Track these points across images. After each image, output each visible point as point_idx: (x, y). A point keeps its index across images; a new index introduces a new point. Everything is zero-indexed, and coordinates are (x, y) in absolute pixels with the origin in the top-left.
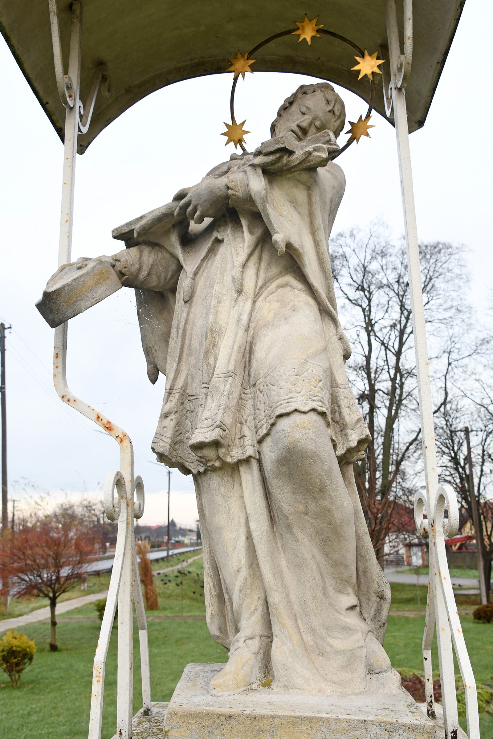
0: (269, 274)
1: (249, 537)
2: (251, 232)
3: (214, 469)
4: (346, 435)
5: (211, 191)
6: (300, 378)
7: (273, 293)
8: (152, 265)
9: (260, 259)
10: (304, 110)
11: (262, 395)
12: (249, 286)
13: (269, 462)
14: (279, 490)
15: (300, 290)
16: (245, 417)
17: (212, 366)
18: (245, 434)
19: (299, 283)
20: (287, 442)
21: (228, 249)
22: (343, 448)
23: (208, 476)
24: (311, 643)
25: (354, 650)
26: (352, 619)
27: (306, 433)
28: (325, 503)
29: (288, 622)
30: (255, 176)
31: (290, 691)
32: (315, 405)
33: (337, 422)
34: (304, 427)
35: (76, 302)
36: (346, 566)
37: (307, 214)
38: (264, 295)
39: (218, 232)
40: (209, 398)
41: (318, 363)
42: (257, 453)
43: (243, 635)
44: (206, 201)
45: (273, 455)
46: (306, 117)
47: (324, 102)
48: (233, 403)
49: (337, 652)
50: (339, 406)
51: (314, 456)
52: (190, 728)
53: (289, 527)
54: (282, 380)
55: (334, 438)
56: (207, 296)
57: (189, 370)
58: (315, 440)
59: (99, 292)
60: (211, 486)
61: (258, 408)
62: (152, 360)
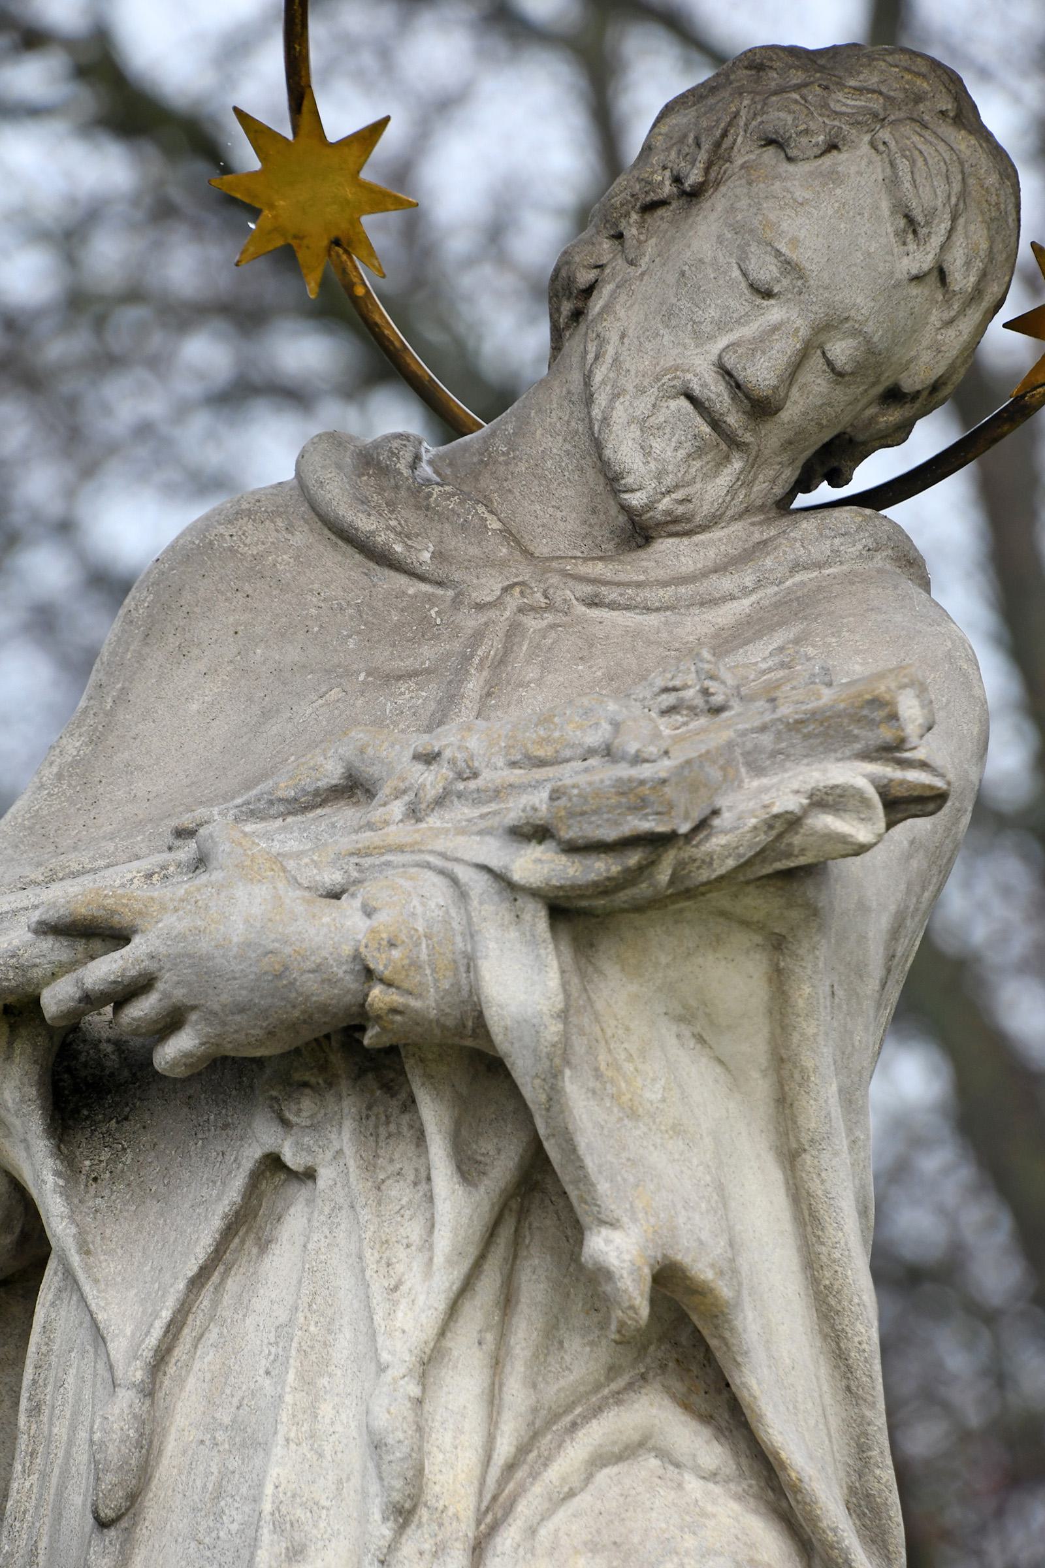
46: (775, 313)
47: (890, 225)
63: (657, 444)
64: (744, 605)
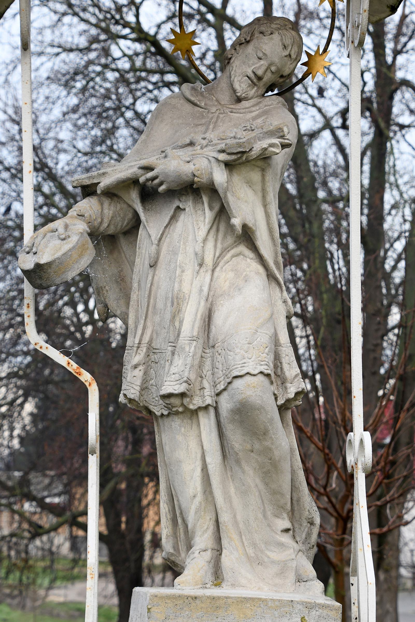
0: (226, 245)
1: (205, 468)
2: (211, 208)
3: (177, 413)
4: (286, 388)
5: (179, 176)
6: (251, 346)
7: (228, 262)
8: (112, 217)
9: (218, 230)
10: (260, 55)
11: (220, 357)
12: (209, 259)
13: (225, 411)
14: (232, 433)
15: (252, 259)
16: (205, 372)
17: (177, 328)
18: (204, 386)
19: (251, 252)
20: (240, 397)
21: (190, 219)
22: (283, 399)
23: (170, 418)
24: (253, 555)
25: (287, 561)
26: (286, 539)
27: (255, 392)
28: (268, 443)
29: (235, 536)
30: (219, 169)
31: (237, 588)
32: (263, 368)
33: (279, 376)
34: (254, 387)
35: (64, 272)
36: (282, 495)
37: (261, 190)
38: (221, 264)
39: (180, 201)
40: (176, 356)
41: (265, 332)
42: (214, 403)
43: (198, 548)
44: (173, 182)
45: (228, 405)
46: (262, 62)
47: (281, 47)
48: (196, 362)
49: (273, 562)
50: (281, 363)
51: (261, 409)
52: (166, 606)
53: (238, 462)
54: (237, 347)
55: (276, 392)
56: (170, 261)
57: (154, 326)
58: (261, 397)
59: (82, 263)
60: (173, 427)
61: (217, 367)
62: (103, 299)
63: (242, 85)
64: (257, 112)
